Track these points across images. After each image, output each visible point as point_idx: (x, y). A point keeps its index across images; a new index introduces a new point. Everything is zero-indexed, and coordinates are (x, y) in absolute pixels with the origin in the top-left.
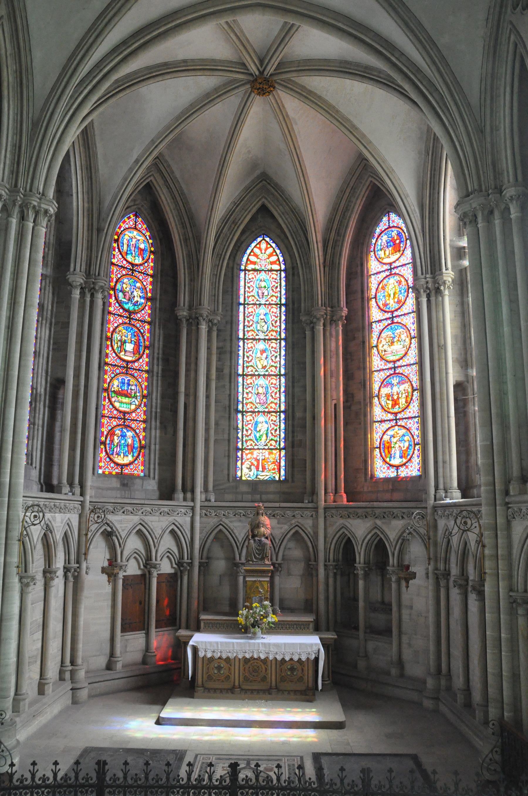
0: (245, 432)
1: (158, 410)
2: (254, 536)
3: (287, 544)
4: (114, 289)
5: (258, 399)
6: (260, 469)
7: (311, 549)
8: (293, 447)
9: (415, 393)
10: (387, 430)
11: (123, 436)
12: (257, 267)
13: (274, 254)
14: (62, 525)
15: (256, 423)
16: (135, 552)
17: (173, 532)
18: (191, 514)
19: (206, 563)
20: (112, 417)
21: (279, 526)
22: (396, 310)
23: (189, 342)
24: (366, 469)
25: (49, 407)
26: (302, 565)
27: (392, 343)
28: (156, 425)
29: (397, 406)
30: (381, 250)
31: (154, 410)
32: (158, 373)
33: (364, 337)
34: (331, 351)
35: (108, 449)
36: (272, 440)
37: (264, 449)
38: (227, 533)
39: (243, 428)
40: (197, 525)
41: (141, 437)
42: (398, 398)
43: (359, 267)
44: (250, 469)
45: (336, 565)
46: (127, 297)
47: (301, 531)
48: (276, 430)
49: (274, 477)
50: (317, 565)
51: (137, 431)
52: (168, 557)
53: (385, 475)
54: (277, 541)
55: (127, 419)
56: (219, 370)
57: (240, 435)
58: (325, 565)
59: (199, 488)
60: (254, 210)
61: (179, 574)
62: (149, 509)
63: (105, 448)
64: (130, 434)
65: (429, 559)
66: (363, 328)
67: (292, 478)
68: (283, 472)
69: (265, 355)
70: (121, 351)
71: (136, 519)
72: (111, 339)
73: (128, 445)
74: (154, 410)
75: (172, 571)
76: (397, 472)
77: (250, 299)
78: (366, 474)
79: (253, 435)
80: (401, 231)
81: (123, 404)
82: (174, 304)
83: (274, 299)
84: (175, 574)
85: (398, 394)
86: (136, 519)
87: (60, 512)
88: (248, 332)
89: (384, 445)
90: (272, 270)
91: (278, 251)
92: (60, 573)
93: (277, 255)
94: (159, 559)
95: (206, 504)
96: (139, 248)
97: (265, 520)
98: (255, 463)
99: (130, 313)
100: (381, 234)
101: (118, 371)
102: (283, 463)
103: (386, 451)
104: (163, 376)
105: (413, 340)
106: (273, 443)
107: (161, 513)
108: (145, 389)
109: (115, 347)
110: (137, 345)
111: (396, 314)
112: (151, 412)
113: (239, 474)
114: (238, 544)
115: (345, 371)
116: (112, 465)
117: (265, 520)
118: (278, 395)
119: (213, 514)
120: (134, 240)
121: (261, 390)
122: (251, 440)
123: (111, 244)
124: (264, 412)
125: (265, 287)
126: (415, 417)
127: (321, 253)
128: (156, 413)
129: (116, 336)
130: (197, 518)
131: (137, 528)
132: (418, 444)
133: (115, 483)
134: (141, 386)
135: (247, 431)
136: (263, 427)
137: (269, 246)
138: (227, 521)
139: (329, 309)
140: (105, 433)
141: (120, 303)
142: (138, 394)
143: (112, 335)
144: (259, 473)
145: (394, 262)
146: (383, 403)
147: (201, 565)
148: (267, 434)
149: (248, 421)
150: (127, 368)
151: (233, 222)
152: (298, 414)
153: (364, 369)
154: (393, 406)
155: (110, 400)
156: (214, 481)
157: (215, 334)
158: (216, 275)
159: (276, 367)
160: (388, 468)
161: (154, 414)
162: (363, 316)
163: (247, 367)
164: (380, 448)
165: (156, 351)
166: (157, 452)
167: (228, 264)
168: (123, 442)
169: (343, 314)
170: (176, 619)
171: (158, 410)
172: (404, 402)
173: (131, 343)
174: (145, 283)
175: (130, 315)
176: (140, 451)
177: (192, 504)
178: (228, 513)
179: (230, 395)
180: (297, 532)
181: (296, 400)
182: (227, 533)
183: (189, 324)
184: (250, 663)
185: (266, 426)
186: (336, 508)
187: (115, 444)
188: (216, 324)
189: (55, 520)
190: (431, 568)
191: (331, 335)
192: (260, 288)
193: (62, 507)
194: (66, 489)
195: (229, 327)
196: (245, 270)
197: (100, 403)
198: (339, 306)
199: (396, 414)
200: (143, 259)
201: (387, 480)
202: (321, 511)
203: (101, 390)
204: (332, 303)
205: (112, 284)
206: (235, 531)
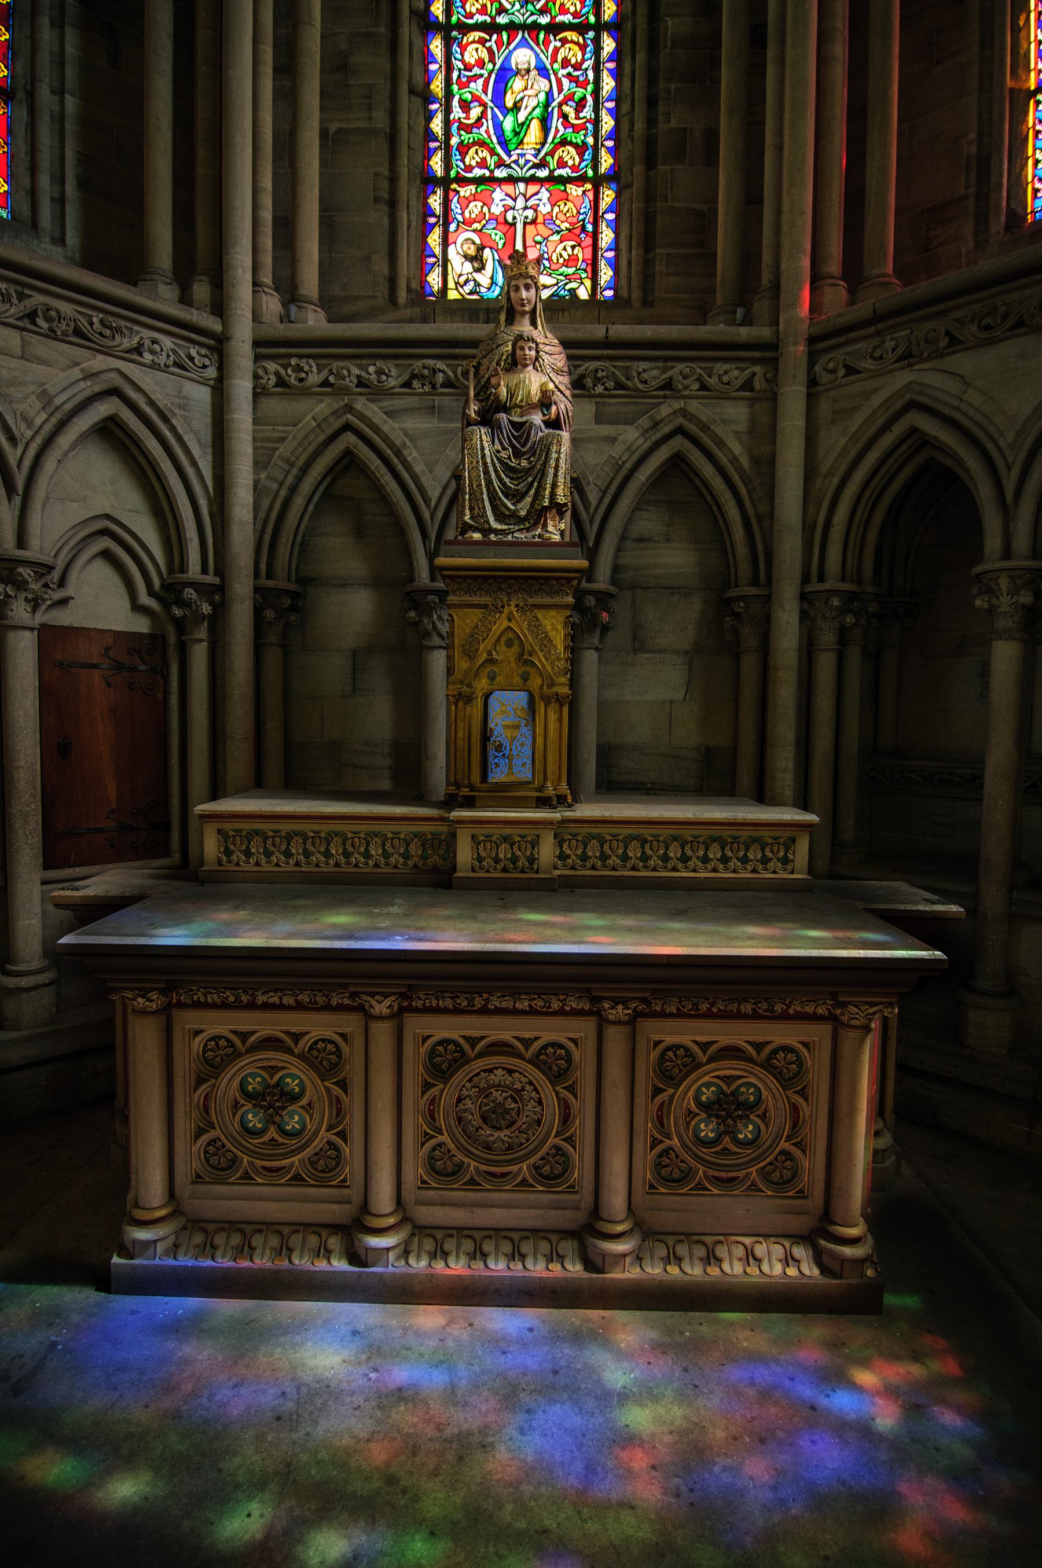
0: (457, 113)
3: (630, 521)
7: (739, 533)
8: (650, 163)
15: (505, 75)
18: (212, 373)
19: (295, 596)
21: (605, 430)
26: (694, 607)
36: (564, 142)
37: (533, 180)
38: (375, 463)
39: (449, 95)
44: (477, 260)
48: (581, 105)
49: (573, 291)
50: (768, 599)
52: (106, 555)
54: (593, 496)
57: (437, 125)
58: (803, 597)
61: (172, 640)
67: (647, 288)
68: (606, 274)
75: (141, 625)
78: (982, 220)
79: (488, 124)
84: (155, 641)
95: (283, 330)
98: (498, 237)
102: (607, 236)
106: (569, 154)
113: (434, 279)
114: (426, 514)
122: (481, 144)
124: (534, 28)
130: (242, 387)
135: (465, 106)
136: (529, 93)
138: (373, 410)
147: (264, 598)
148: (545, 123)
149: (468, 67)
166: (69, 127)
170: (167, 827)
178: (380, 372)
180: (677, 463)
182: (375, 463)
184: (459, 1078)
185: (543, 84)
202: (796, 351)
206: (412, 455)
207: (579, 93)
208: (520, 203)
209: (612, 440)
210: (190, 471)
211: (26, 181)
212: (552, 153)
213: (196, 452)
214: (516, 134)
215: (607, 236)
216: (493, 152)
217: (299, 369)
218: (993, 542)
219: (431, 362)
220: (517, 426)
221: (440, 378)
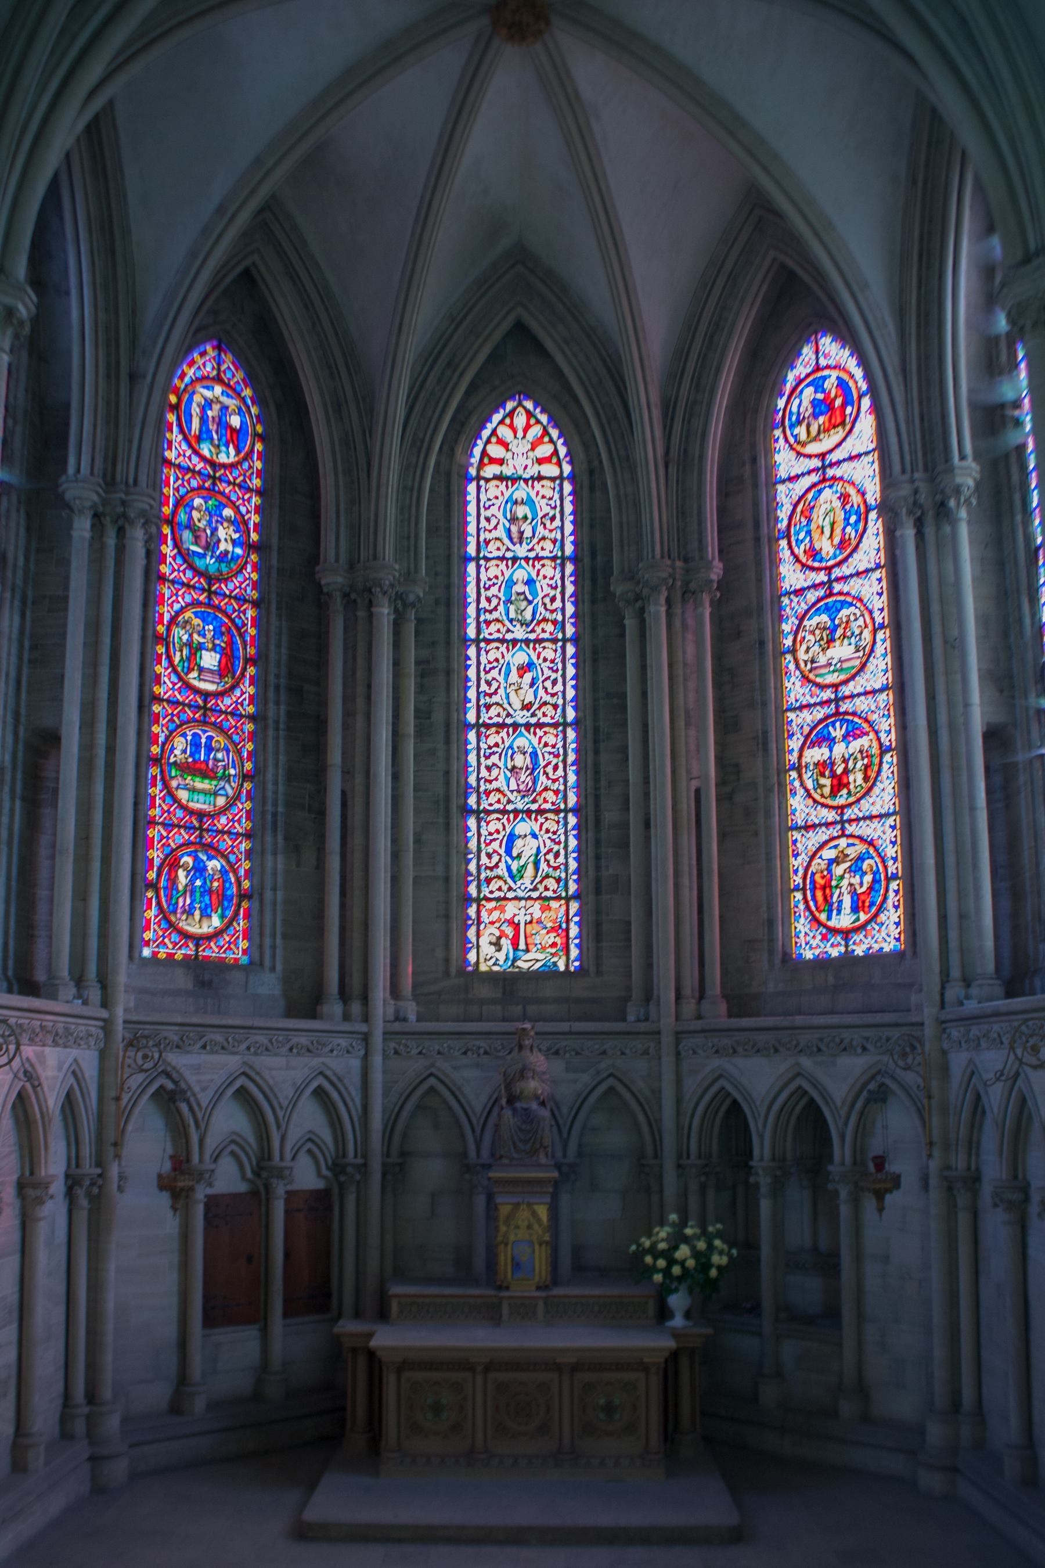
0: (484, 860)
1: (280, 809)
2: (511, 1100)
4: (171, 521)
5: (513, 781)
6: (522, 945)
7: (645, 1129)
8: (598, 892)
9: (887, 758)
10: (821, 847)
11: (199, 869)
12: (508, 471)
13: (546, 439)
14: (61, 1075)
15: (512, 838)
16: (233, 1141)
17: (319, 1093)
18: (362, 1052)
19: (401, 1165)
20: (173, 826)
22: (839, 564)
23: (350, 647)
24: (772, 940)
25: (23, 799)
27: (831, 641)
28: (275, 844)
29: (844, 791)
30: (799, 422)
31: (269, 808)
32: (277, 722)
33: (761, 630)
34: (685, 664)
35: (163, 900)
37: (530, 898)
38: (447, 1094)
39: (479, 851)
40: (377, 1077)
41: (242, 872)
42: (846, 771)
43: (748, 467)
44: (497, 945)
45: (706, 1165)
46: (203, 542)
47: (620, 1089)
48: (557, 855)
49: (555, 964)
50: (661, 1166)
51: (232, 858)
53: (817, 952)
54: (565, 1110)
55: (208, 830)
56: (423, 715)
57: (472, 867)
59: (380, 992)
60: (497, 336)
62: (262, 1039)
63: (158, 897)
64: (214, 865)
65: (931, 1144)
66: (760, 608)
67: (598, 965)
68: (574, 952)
69: (528, 677)
70: (190, 670)
71: (232, 1062)
72: (164, 640)
73: (210, 892)
74: (269, 808)
76: (847, 946)
77: (492, 547)
78: (771, 952)
79: (502, 865)
80: (845, 377)
81: (196, 794)
82: (314, 559)
83: (548, 545)
85: (845, 761)
86: (232, 1062)
87: (56, 1044)
88: (488, 623)
89: (813, 882)
90: (540, 478)
91: (554, 433)
92: (58, 1187)
93: (551, 441)
94: (288, 1156)
95: (397, 1026)
96: (229, 426)
97: (537, 1060)
98: (510, 931)
99: (210, 579)
100: (797, 385)
101: (184, 717)
102: (574, 931)
103: (819, 894)
104: (288, 729)
105: (880, 635)
106: (551, 883)
107: (291, 1049)
108: (249, 759)
109: (177, 659)
110: (228, 656)
111: (837, 572)
112: (263, 813)
113: (472, 957)
114: (475, 1121)
115: (720, 711)
116: (175, 937)
117: (537, 1060)
118: (560, 772)
119: (415, 1051)
120: (216, 407)
121: (519, 761)
122: (499, 877)
123: (161, 417)
124: (529, 812)
125: (525, 518)
126: (888, 815)
127: (658, 433)
128: (275, 815)
129: (180, 634)
130: (377, 1060)
131: (237, 1084)
132: (895, 877)
133: (183, 980)
134: (240, 752)
136: (526, 848)
137: (532, 421)
139: (679, 564)
140: (157, 862)
141: (185, 556)
142: (232, 772)
143: (169, 630)
144: (521, 953)
145: (831, 451)
146: (810, 784)
148: (536, 864)
150: (204, 711)
151: (449, 364)
152: (610, 816)
153: (764, 704)
154: (834, 792)
155: (166, 785)
156: (414, 973)
157: (410, 628)
158: (412, 489)
159: (555, 707)
160: (824, 938)
161: (269, 817)
162: (759, 580)
163: (488, 707)
164: (804, 890)
165: (273, 670)
166: (279, 908)
167: (438, 464)
168: (198, 883)
169: (714, 577)
171: (280, 809)
172: (860, 781)
173: (214, 649)
174: (243, 510)
175: (210, 585)
176: (239, 906)
177: (363, 1028)
179: (447, 773)
181: (603, 783)
182: (447, 1094)
183: (350, 604)
186: (703, 1031)
187: (180, 887)
188: (413, 605)
189: (43, 1063)
190: (934, 1165)
191: (684, 626)
192: (514, 520)
193: (61, 1031)
194: (69, 991)
195: (441, 610)
196: (479, 478)
197: (142, 790)
198: (702, 558)
199: (842, 808)
200: (238, 451)
201: (822, 963)
202: (667, 1039)
203: (144, 761)
204: (685, 549)
205: (167, 510)
207: (556, 848)
208: (523, 911)
209: (575, 1081)
210: (350, 1104)
211: (257, 940)
212: (541, 882)
213: (354, 1093)
214: (520, 872)
215: (574, 931)
216: (505, 882)
217: (406, 1046)
218: (756, 1152)
219: (477, 1043)
220: (526, 1110)
221: (482, 1051)
